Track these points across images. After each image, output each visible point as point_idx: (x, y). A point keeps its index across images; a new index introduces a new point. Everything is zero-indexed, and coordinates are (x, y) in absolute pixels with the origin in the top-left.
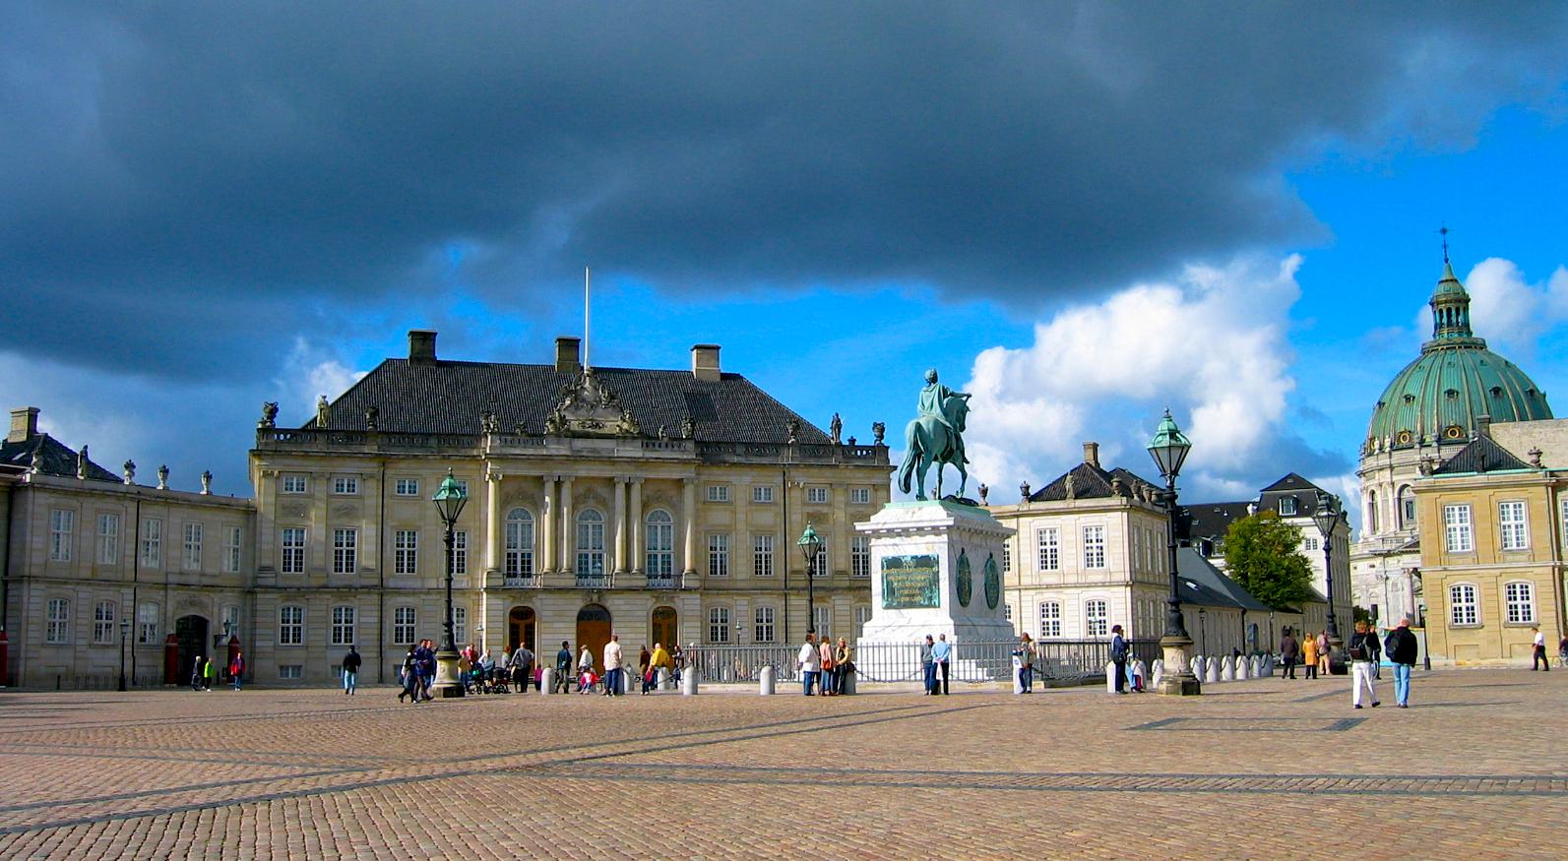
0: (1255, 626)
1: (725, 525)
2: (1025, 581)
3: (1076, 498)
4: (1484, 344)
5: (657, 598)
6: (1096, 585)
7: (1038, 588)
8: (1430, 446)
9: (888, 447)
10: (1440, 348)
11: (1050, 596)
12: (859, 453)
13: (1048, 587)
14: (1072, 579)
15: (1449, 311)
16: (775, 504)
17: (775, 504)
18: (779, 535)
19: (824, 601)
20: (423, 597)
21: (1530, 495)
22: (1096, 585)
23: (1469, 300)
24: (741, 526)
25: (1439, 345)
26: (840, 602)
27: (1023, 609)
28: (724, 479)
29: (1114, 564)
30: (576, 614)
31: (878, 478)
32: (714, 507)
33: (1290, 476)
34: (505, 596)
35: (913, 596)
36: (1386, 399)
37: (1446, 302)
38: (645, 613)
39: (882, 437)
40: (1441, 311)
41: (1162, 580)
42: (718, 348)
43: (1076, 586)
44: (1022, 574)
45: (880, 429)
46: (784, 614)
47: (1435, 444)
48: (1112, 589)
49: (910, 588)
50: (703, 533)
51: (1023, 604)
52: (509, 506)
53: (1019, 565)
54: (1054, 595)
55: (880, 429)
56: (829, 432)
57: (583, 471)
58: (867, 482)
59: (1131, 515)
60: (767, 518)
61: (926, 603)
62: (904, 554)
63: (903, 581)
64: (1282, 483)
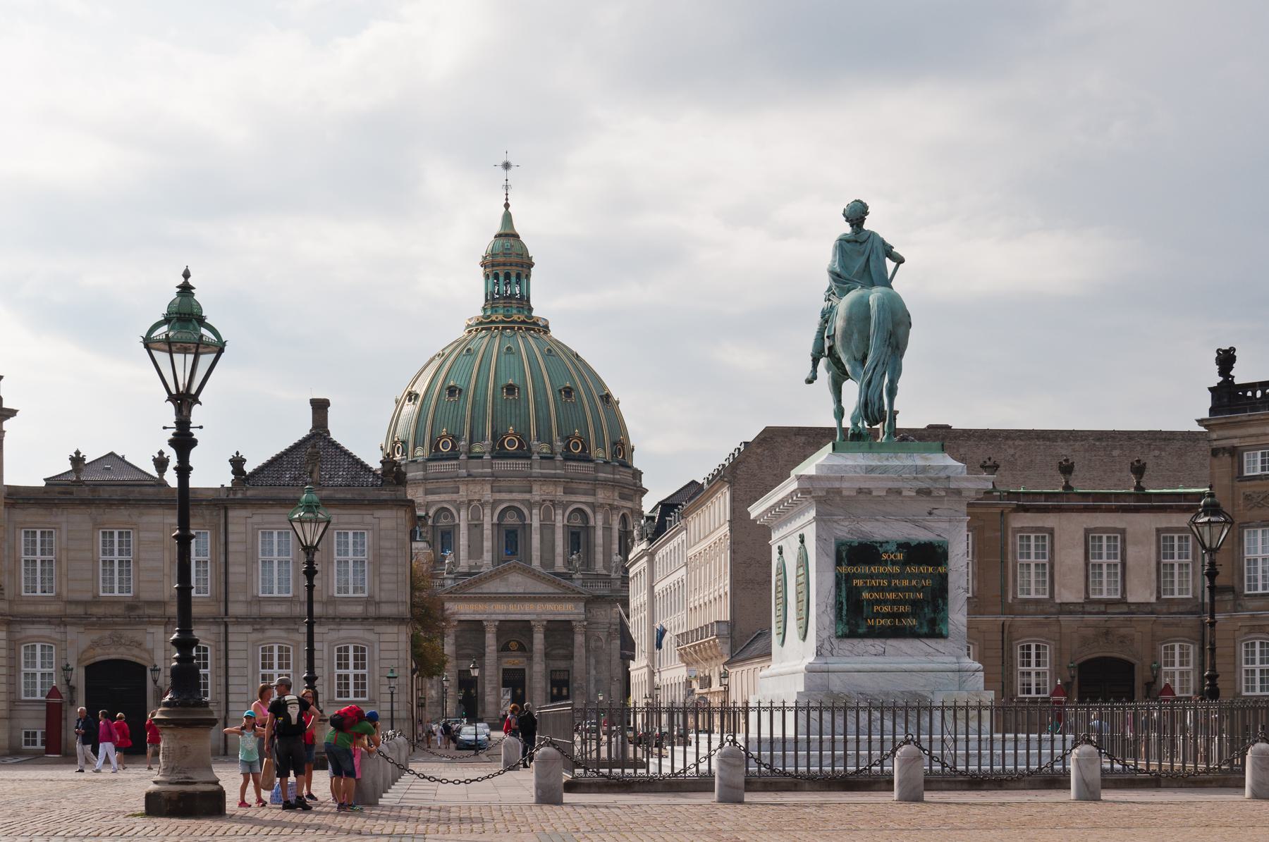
2: (236, 609)
4: (547, 327)
6: (353, 619)
7: (259, 622)
8: (481, 457)
10: (493, 326)
15: (507, 276)
22: (353, 619)
23: (532, 265)
25: (492, 322)
27: (231, 655)
35: (900, 616)
37: (504, 265)
40: (496, 276)
44: (231, 597)
47: (487, 457)
48: (377, 629)
49: (894, 602)
53: (226, 583)
54: (283, 634)
61: (925, 630)
62: (878, 538)
63: (880, 589)
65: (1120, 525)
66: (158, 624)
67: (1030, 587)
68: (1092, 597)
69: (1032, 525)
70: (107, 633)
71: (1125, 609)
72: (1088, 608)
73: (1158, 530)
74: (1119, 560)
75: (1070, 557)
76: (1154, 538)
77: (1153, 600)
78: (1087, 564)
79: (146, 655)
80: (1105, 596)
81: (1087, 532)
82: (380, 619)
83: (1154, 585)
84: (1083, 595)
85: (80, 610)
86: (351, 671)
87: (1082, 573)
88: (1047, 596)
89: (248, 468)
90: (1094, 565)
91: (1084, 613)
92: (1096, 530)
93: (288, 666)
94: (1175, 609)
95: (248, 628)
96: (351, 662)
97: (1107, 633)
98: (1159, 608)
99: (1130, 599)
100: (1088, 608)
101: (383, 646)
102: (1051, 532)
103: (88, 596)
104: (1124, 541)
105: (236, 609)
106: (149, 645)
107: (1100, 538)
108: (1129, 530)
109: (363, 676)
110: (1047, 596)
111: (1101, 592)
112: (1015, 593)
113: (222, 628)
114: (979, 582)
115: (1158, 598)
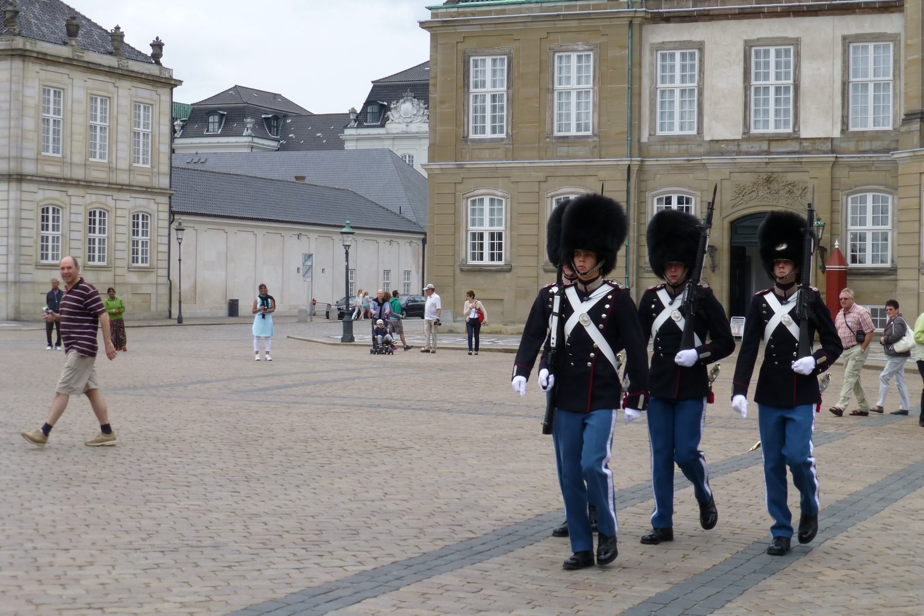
21: (605, 39)
65: (791, 34)
67: (676, 122)
68: (753, 131)
69: (675, 39)
71: (795, 146)
72: (745, 147)
73: (844, 38)
74: (791, 81)
75: (724, 79)
76: (839, 49)
77: (837, 134)
78: (747, 88)
80: (772, 130)
81: (748, 45)
83: (838, 113)
84: (740, 129)
87: (741, 100)
88: (694, 132)
90: (757, 89)
91: (739, 153)
92: (759, 42)
94: (866, 146)
97: (768, 181)
98: (844, 145)
99: (804, 134)
100: (745, 147)
102: (700, 46)
104: (797, 55)
107: (767, 53)
108: (805, 40)
110: (694, 132)
111: (766, 123)
112: (653, 128)
114: (600, 116)
115: (843, 131)
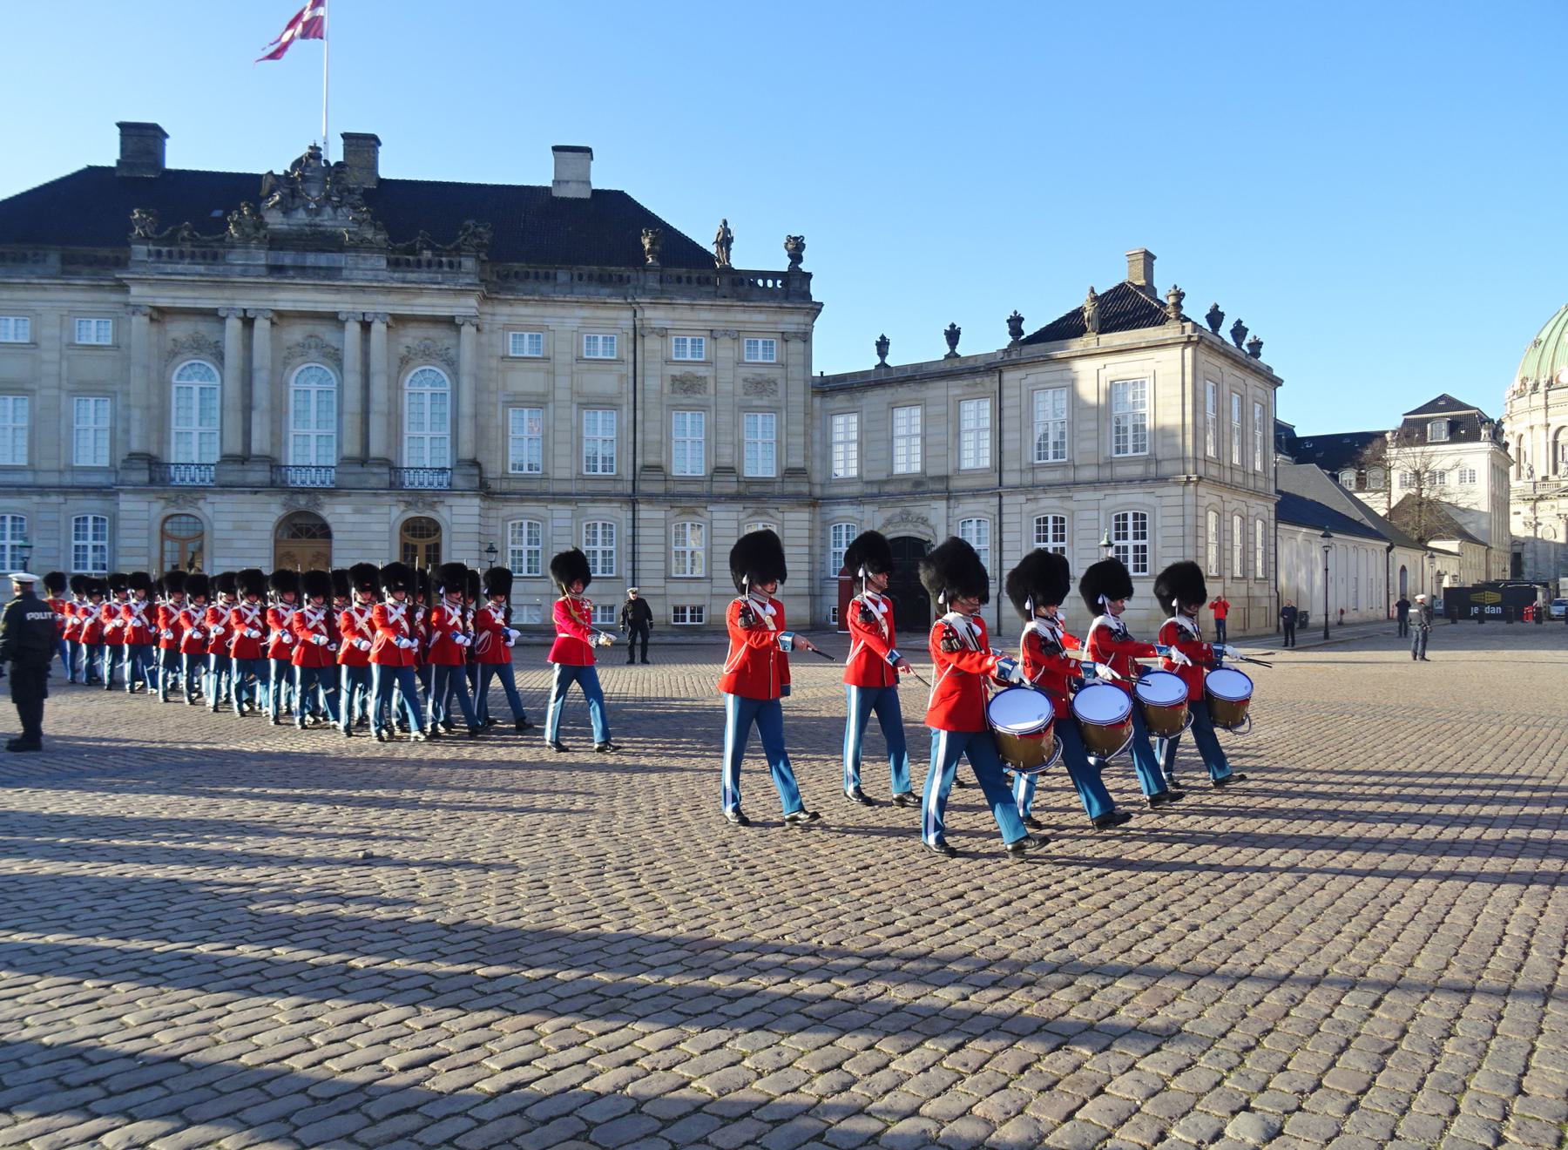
0: (1403, 569)
1: (538, 395)
3: (1102, 331)
5: (408, 504)
7: (1031, 489)
9: (809, 276)
11: (1050, 505)
12: (760, 282)
13: (1049, 486)
14: (1087, 474)
16: (620, 361)
17: (620, 361)
18: (625, 409)
19: (695, 513)
20: (36, 499)
24: (562, 394)
26: (722, 515)
27: (1005, 528)
28: (536, 321)
29: (1163, 446)
30: (270, 526)
31: (791, 321)
32: (519, 365)
33: (1443, 397)
34: (152, 497)
36: (1543, 337)
38: (386, 528)
39: (800, 259)
41: (1261, 484)
42: (588, 150)
43: (1094, 484)
44: (1006, 466)
45: (796, 248)
46: (630, 532)
48: (1159, 491)
50: (500, 408)
51: (1005, 519)
52: (178, 359)
54: (1056, 503)
55: (796, 248)
56: (713, 250)
57: (287, 299)
58: (771, 328)
59: (1202, 357)
60: (608, 383)
64: (1432, 406)
66: (941, 498)
70: (898, 510)
79: (930, 531)
82: (1162, 480)
85: (875, 490)
86: (1131, 542)
89: (1029, 329)
93: (1063, 539)
95: (1022, 498)
96: (1130, 531)
101: (1166, 511)
103: (882, 476)
105: (1010, 479)
106: (932, 521)
109: (1144, 548)
113: (995, 501)
